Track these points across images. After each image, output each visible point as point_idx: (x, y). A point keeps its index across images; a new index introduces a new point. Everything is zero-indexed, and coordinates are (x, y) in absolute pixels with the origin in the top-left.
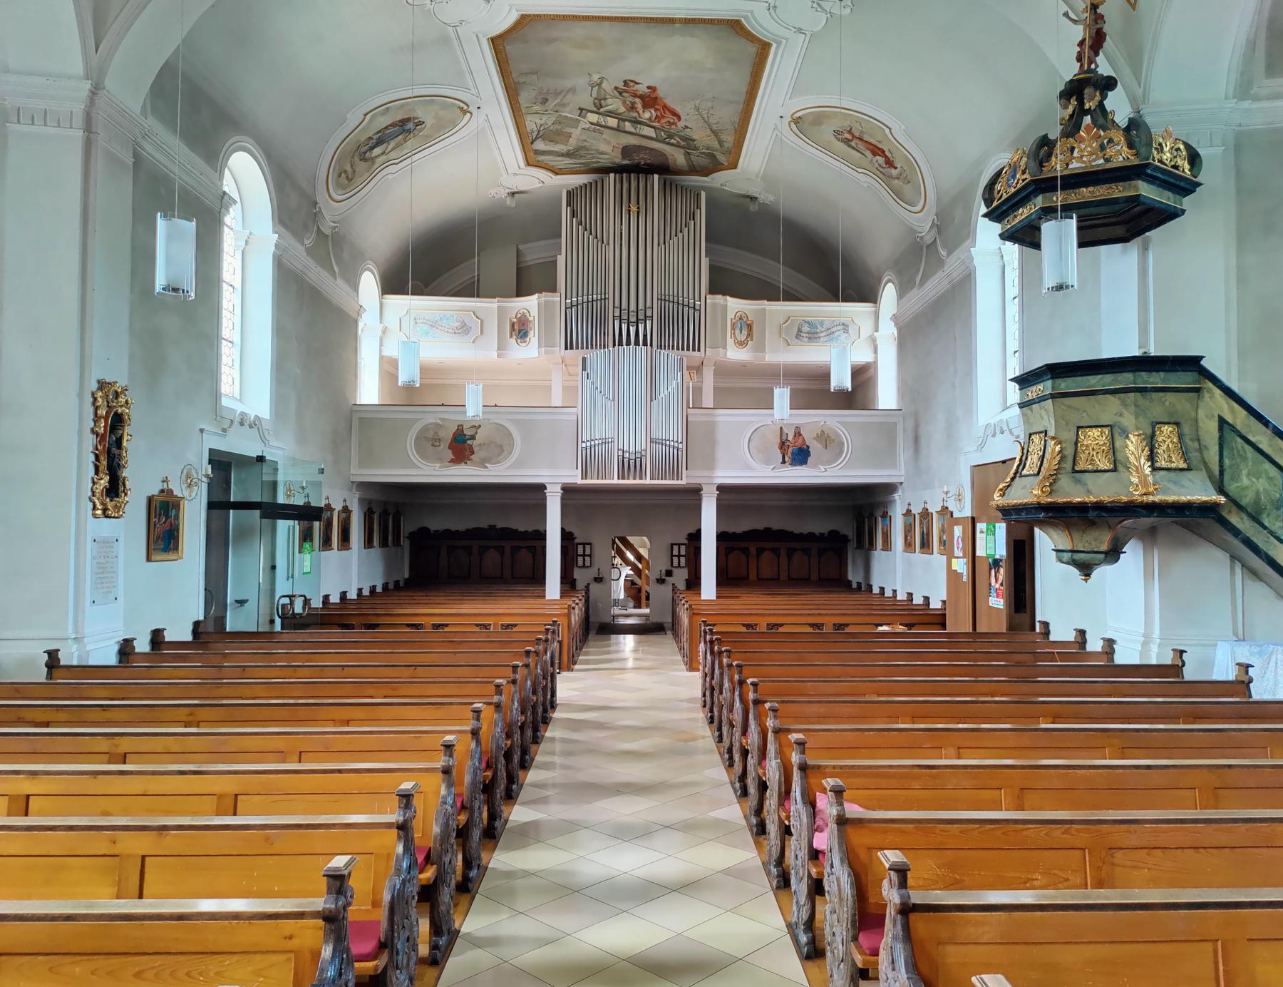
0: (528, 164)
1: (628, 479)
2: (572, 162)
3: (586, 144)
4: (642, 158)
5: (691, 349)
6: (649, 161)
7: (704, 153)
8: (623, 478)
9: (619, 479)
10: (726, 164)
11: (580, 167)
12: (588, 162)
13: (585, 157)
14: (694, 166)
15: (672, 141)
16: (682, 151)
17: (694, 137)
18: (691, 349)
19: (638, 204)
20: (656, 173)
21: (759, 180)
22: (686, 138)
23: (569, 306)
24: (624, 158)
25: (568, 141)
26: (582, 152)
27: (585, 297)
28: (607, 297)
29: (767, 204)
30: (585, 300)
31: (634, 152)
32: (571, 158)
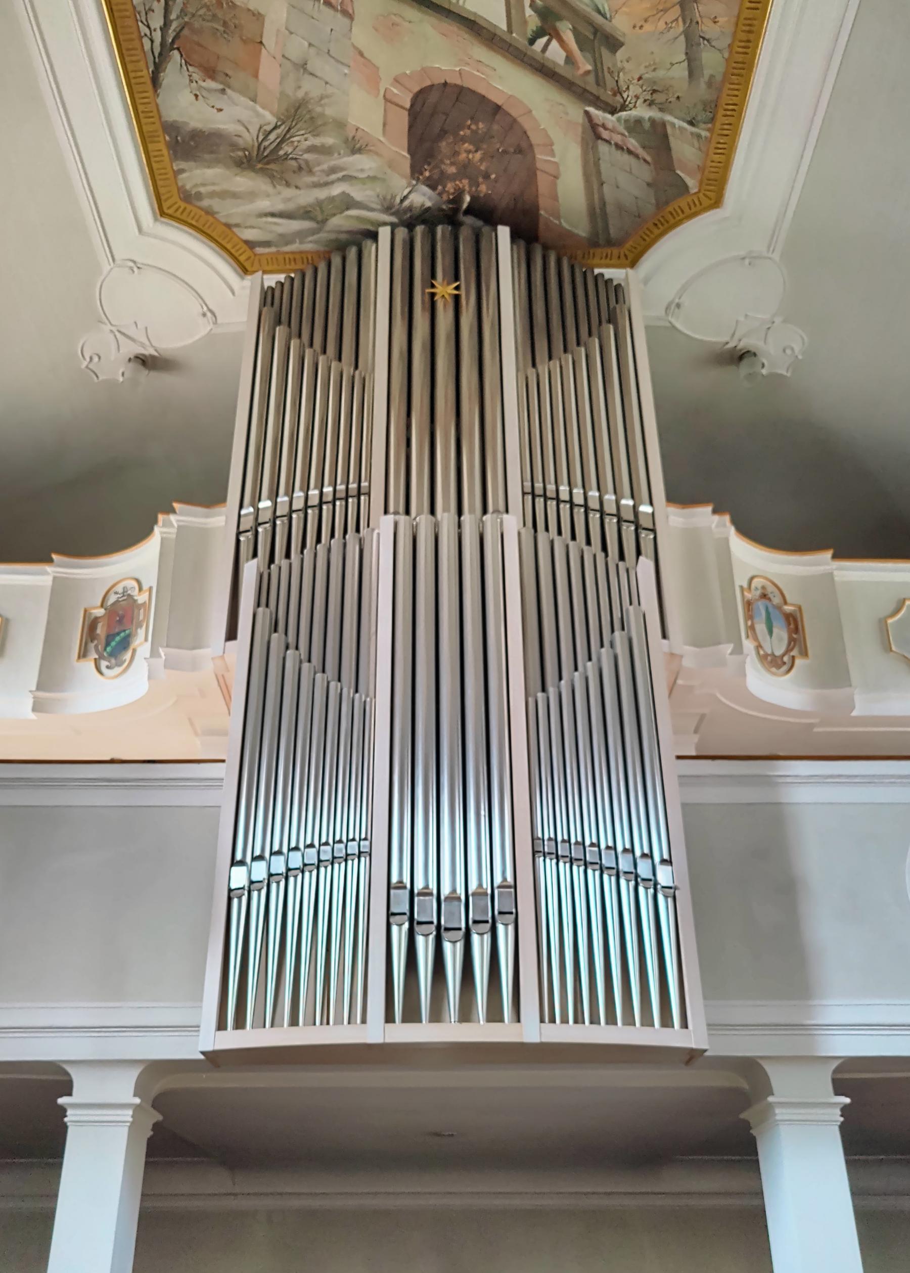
0: (162, 211)
1: (436, 1016)
2: (280, 207)
3: (310, 88)
4: (465, 169)
5: (547, 1019)
6: (483, 188)
7: (635, 126)
8: (412, 1015)
9: (389, 1018)
10: (692, 183)
11: (301, 235)
12: (320, 204)
13: (310, 172)
14: (603, 204)
15: (555, 53)
16: (575, 111)
17: (620, 24)
18: (547, 1019)
19: (457, 278)
20: (504, 224)
21: (776, 256)
22: (596, 30)
23: (247, 523)
24: (416, 171)
25: (256, 76)
26: (302, 140)
27: (299, 494)
28: (364, 484)
29: (781, 375)
30: (298, 504)
31: (443, 133)
32: (272, 177)
